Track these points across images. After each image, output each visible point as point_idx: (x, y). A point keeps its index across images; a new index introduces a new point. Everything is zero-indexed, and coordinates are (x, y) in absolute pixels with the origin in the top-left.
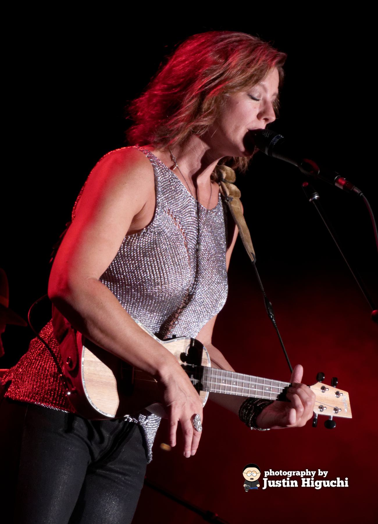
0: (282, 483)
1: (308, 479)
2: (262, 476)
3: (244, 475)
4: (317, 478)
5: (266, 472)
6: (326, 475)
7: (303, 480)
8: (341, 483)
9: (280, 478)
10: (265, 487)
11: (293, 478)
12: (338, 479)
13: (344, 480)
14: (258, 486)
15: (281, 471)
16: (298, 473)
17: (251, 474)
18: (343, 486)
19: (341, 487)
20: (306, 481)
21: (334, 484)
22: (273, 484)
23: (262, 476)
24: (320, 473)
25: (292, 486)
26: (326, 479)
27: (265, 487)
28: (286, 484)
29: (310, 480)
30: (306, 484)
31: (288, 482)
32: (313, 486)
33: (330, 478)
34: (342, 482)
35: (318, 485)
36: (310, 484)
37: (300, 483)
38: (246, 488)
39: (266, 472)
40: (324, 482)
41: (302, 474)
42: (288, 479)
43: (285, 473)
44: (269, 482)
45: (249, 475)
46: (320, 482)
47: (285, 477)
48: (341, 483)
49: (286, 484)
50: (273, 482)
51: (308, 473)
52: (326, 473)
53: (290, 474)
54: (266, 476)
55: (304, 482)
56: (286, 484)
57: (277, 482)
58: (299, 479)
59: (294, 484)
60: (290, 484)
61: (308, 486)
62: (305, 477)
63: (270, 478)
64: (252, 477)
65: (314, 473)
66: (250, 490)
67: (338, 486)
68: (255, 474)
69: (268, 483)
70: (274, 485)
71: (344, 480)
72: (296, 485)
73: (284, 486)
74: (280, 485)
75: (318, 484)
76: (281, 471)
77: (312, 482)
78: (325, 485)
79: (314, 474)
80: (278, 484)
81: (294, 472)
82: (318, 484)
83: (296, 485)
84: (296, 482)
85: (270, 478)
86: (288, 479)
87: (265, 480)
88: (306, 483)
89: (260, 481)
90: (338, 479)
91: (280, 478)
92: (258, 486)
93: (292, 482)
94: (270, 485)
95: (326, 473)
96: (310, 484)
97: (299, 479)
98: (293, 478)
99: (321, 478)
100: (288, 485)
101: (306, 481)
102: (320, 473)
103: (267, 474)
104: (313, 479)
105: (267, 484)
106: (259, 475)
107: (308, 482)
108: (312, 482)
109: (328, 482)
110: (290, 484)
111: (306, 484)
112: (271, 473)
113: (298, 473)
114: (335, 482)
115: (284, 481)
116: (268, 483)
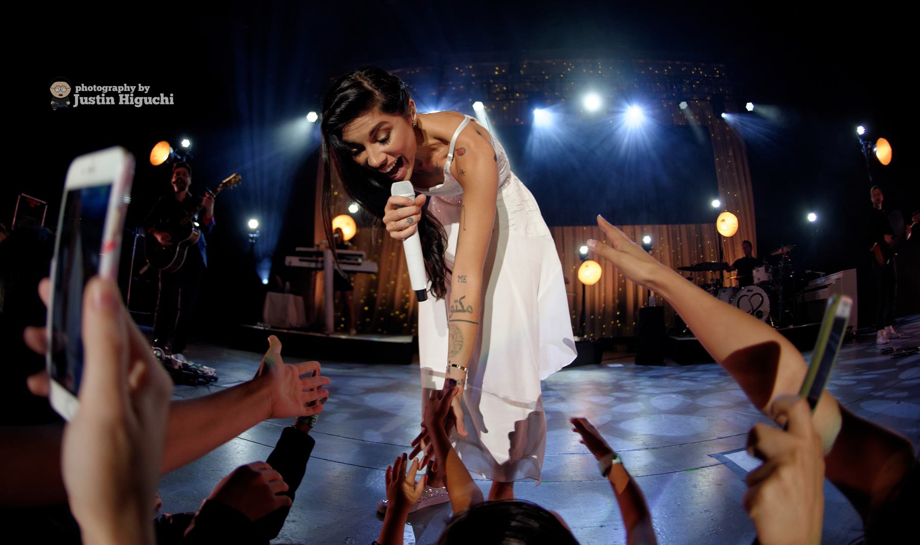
1: (127, 96)
2: (73, 91)
4: (137, 94)
7: (121, 96)
8: (165, 100)
9: (94, 94)
10: (76, 105)
11: (109, 94)
12: (162, 95)
13: (169, 97)
14: (68, 103)
16: (115, 89)
17: (60, 89)
18: (167, 103)
22: (85, 101)
23: (73, 91)
24: (141, 88)
25: (108, 103)
26: (147, 95)
27: (76, 105)
28: (101, 100)
31: (103, 99)
32: (132, 103)
33: (152, 94)
34: (166, 98)
35: (139, 102)
37: (117, 100)
40: (146, 98)
41: (120, 89)
43: (100, 88)
44: (81, 98)
46: (141, 99)
47: (100, 93)
48: (165, 100)
49: (101, 101)
50: (86, 98)
51: (126, 88)
52: (147, 88)
53: (105, 89)
55: (121, 99)
56: (101, 101)
57: (90, 98)
58: (116, 95)
59: (111, 101)
61: (127, 103)
62: (123, 92)
63: (82, 94)
65: (133, 88)
66: (58, 108)
67: (162, 103)
70: (86, 103)
71: (169, 97)
72: (113, 103)
73: (98, 103)
74: (94, 103)
77: (132, 99)
78: (146, 103)
80: (91, 101)
84: (112, 99)
85: (82, 94)
87: (76, 96)
88: (124, 100)
89: (71, 97)
90: (162, 95)
91: (94, 94)
92: (68, 103)
93: (108, 99)
94: (82, 103)
95: (147, 88)
97: (116, 95)
98: (109, 94)
99: (142, 94)
100: (103, 103)
102: (141, 88)
103: (78, 89)
106: (69, 90)
107: (127, 99)
108: (132, 99)
109: (150, 98)
112: (83, 88)
113: (115, 89)
115: (98, 97)
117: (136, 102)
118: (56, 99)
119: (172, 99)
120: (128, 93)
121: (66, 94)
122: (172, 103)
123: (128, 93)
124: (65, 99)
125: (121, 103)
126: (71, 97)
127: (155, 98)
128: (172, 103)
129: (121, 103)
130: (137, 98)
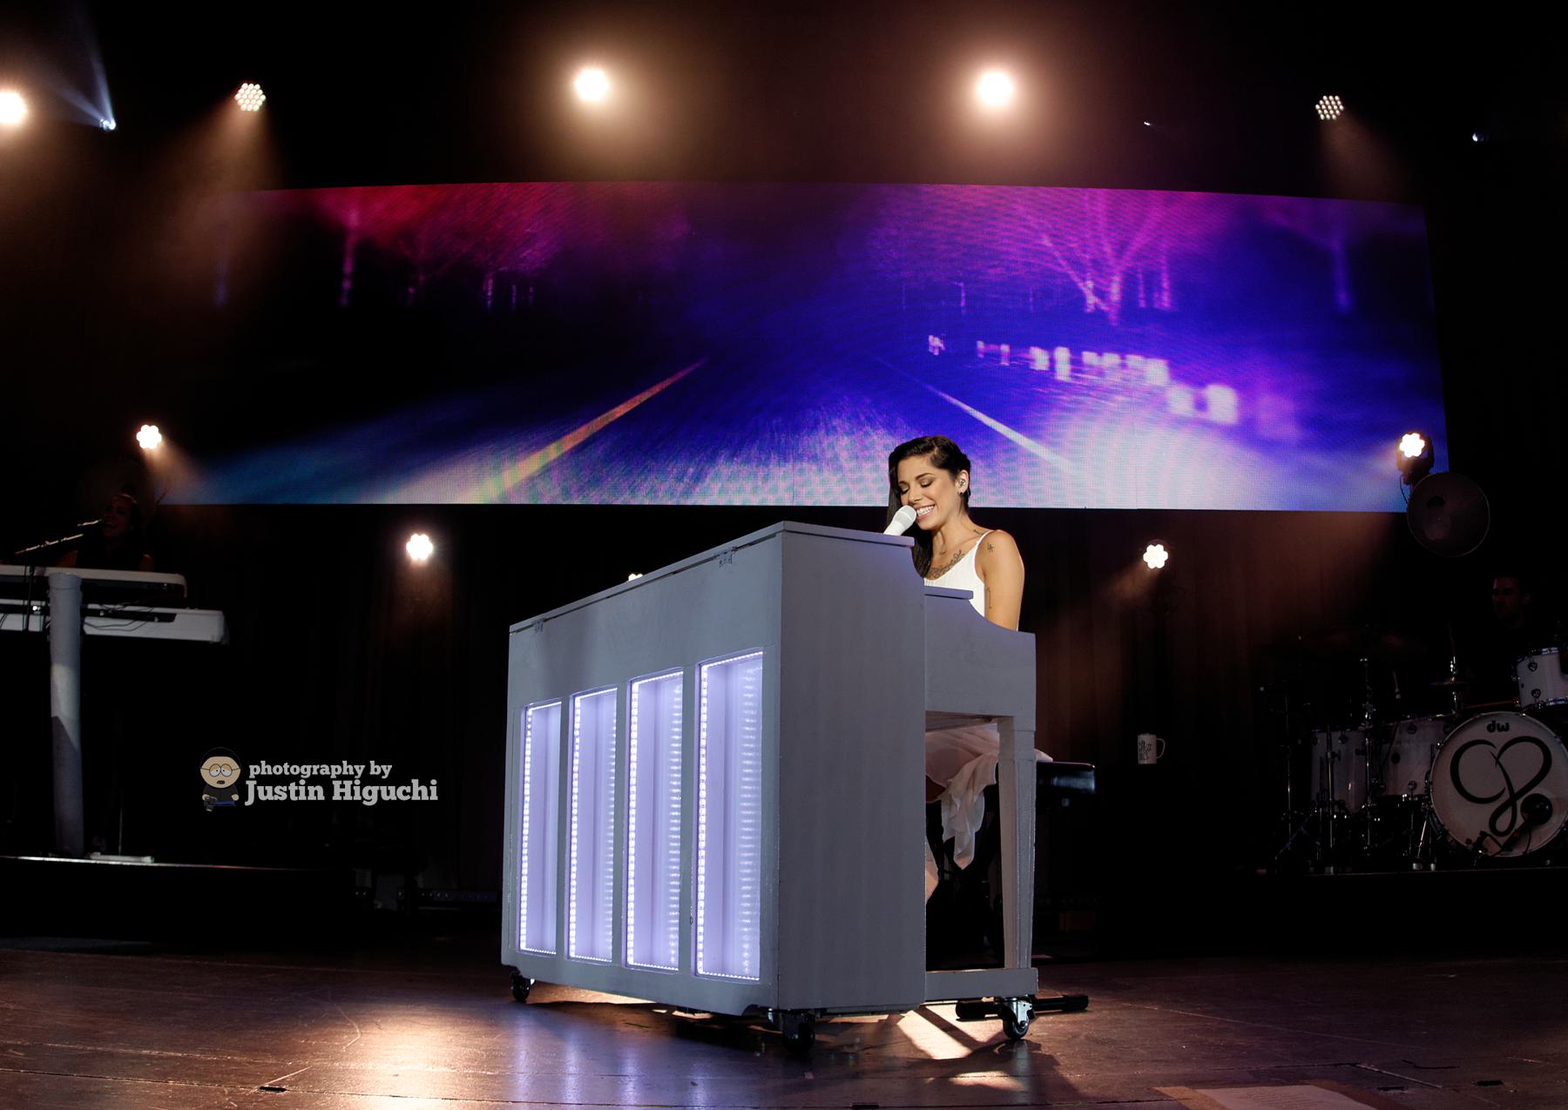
0: (288, 792)
3: (204, 773)
5: (252, 767)
6: (387, 773)
11: (313, 781)
15: (286, 766)
17: (219, 771)
20: (342, 786)
21: (405, 793)
29: (355, 785)
30: (342, 794)
31: (302, 790)
34: (424, 789)
36: (353, 793)
38: (209, 802)
39: (252, 767)
42: (302, 782)
44: (261, 789)
45: (214, 773)
49: (297, 793)
54: (252, 775)
55: (337, 790)
56: (297, 793)
57: (277, 789)
60: (307, 793)
64: (221, 778)
66: (216, 809)
68: (227, 772)
75: (370, 793)
76: (286, 766)
77: (357, 789)
79: (360, 773)
81: (316, 767)
82: (370, 793)
83: (321, 797)
86: (302, 782)
96: (353, 793)
98: (313, 781)
101: (342, 786)
104: (357, 782)
105: (257, 793)
108: (357, 789)
109: (392, 789)
110: (307, 793)
111: (342, 794)
114: (408, 789)
115: (293, 787)
120: (351, 778)
121: (230, 781)
122: (434, 797)
123: (351, 778)
126: (240, 787)
127: (401, 788)
128: (434, 797)
130: (366, 789)
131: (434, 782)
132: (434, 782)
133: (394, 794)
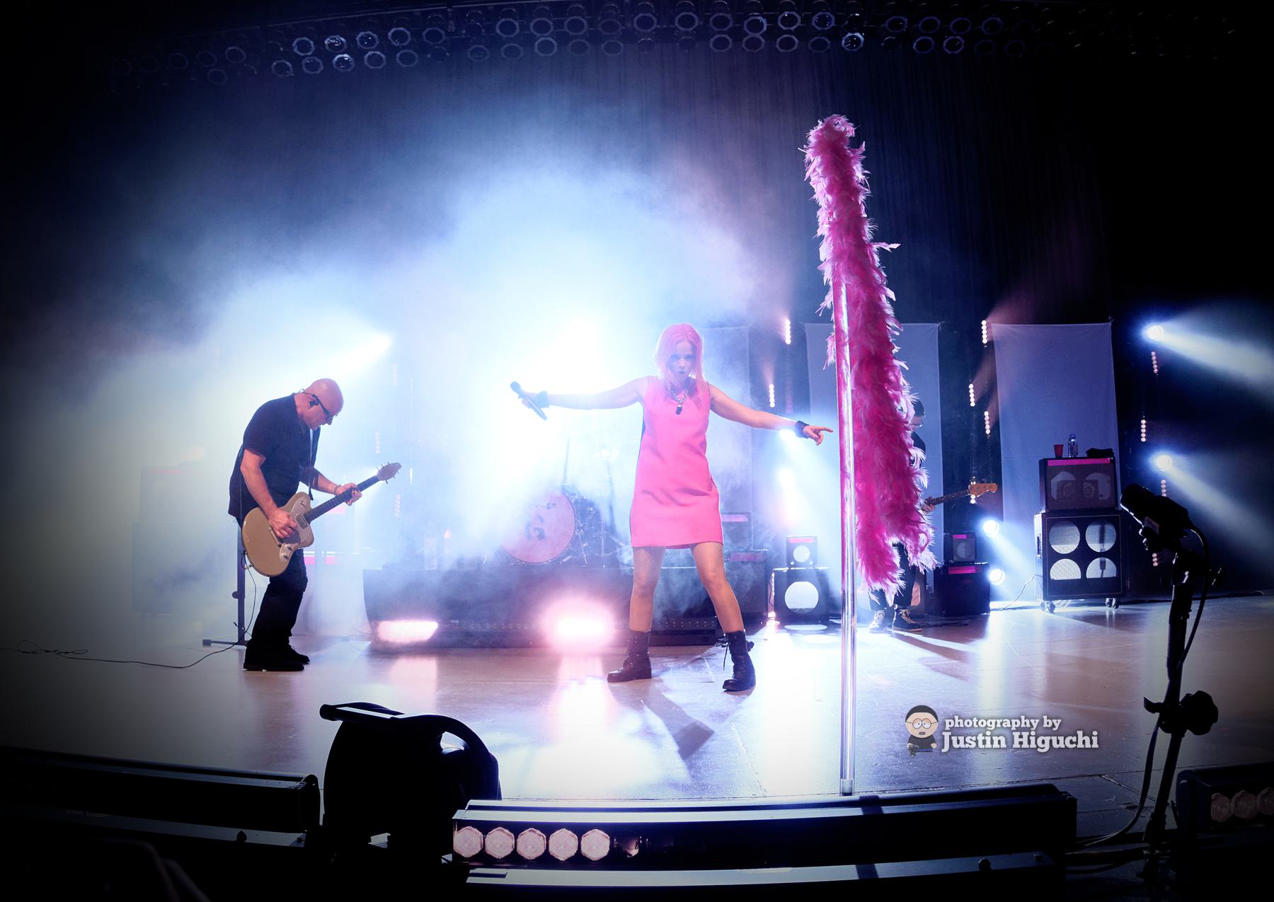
0: (977, 741)
1: (1025, 734)
3: (909, 726)
6: (1057, 725)
7: (1016, 735)
12: (1080, 733)
15: (975, 720)
18: (1088, 745)
19: (1085, 749)
20: (1021, 737)
21: (1071, 742)
25: (996, 745)
26: (1057, 734)
30: (1021, 743)
31: (988, 739)
32: (1033, 745)
34: (1087, 739)
36: (1029, 742)
37: (1010, 741)
40: (1054, 739)
45: (916, 726)
46: (1047, 739)
49: (984, 742)
50: (961, 739)
54: (947, 727)
55: (1017, 740)
56: (984, 742)
57: (968, 739)
60: (992, 742)
61: (1025, 745)
62: (1018, 729)
64: (922, 730)
67: (1080, 745)
68: (927, 725)
69: (951, 742)
72: (1003, 745)
73: (981, 745)
75: (1043, 742)
76: (975, 720)
77: (1033, 739)
78: (1055, 745)
79: (1035, 725)
82: (1043, 742)
84: (1002, 739)
86: (988, 733)
87: (947, 735)
90: (1080, 733)
94: (955, 745)
95: (1057, 723)
96: (1029, 742)
99: (1050, 732)
101: (1021, 737)
104: (1033, 733)
106: (935, 727)
107: (1025, 740)
108: (1033, 739)
109: (1061, 739)
110: (992, 742)
111: (1021, 743)
113: (1007, 723)
114: (1074, 739)
116: (951, 742)
117: (1040, 744)
118: (913, 739)
119: (1095, 739)
120: (1028, 730)
122: (1095, 745)
123: (1028, 730)
124: (931, 739)
125: (1016, 745)
127: (1069, 738)
129: (1016, 745)
130: (1040, 739)
131: (1095, 733)
132: (1095, 733)
133: (1063, 743)
